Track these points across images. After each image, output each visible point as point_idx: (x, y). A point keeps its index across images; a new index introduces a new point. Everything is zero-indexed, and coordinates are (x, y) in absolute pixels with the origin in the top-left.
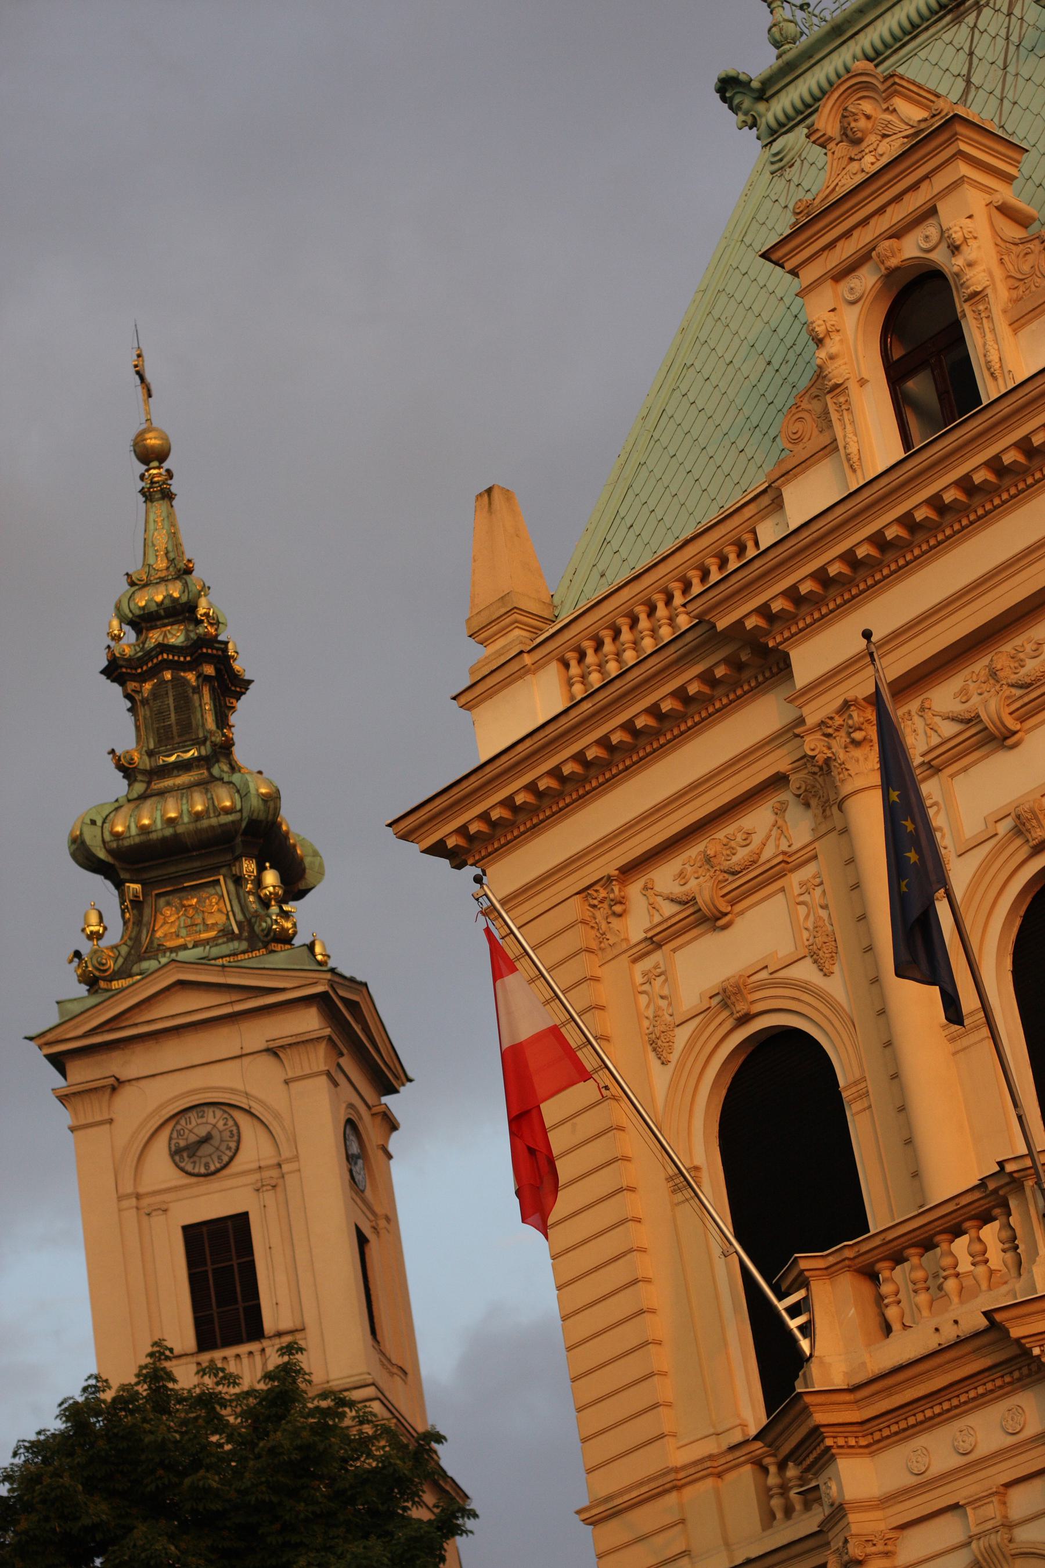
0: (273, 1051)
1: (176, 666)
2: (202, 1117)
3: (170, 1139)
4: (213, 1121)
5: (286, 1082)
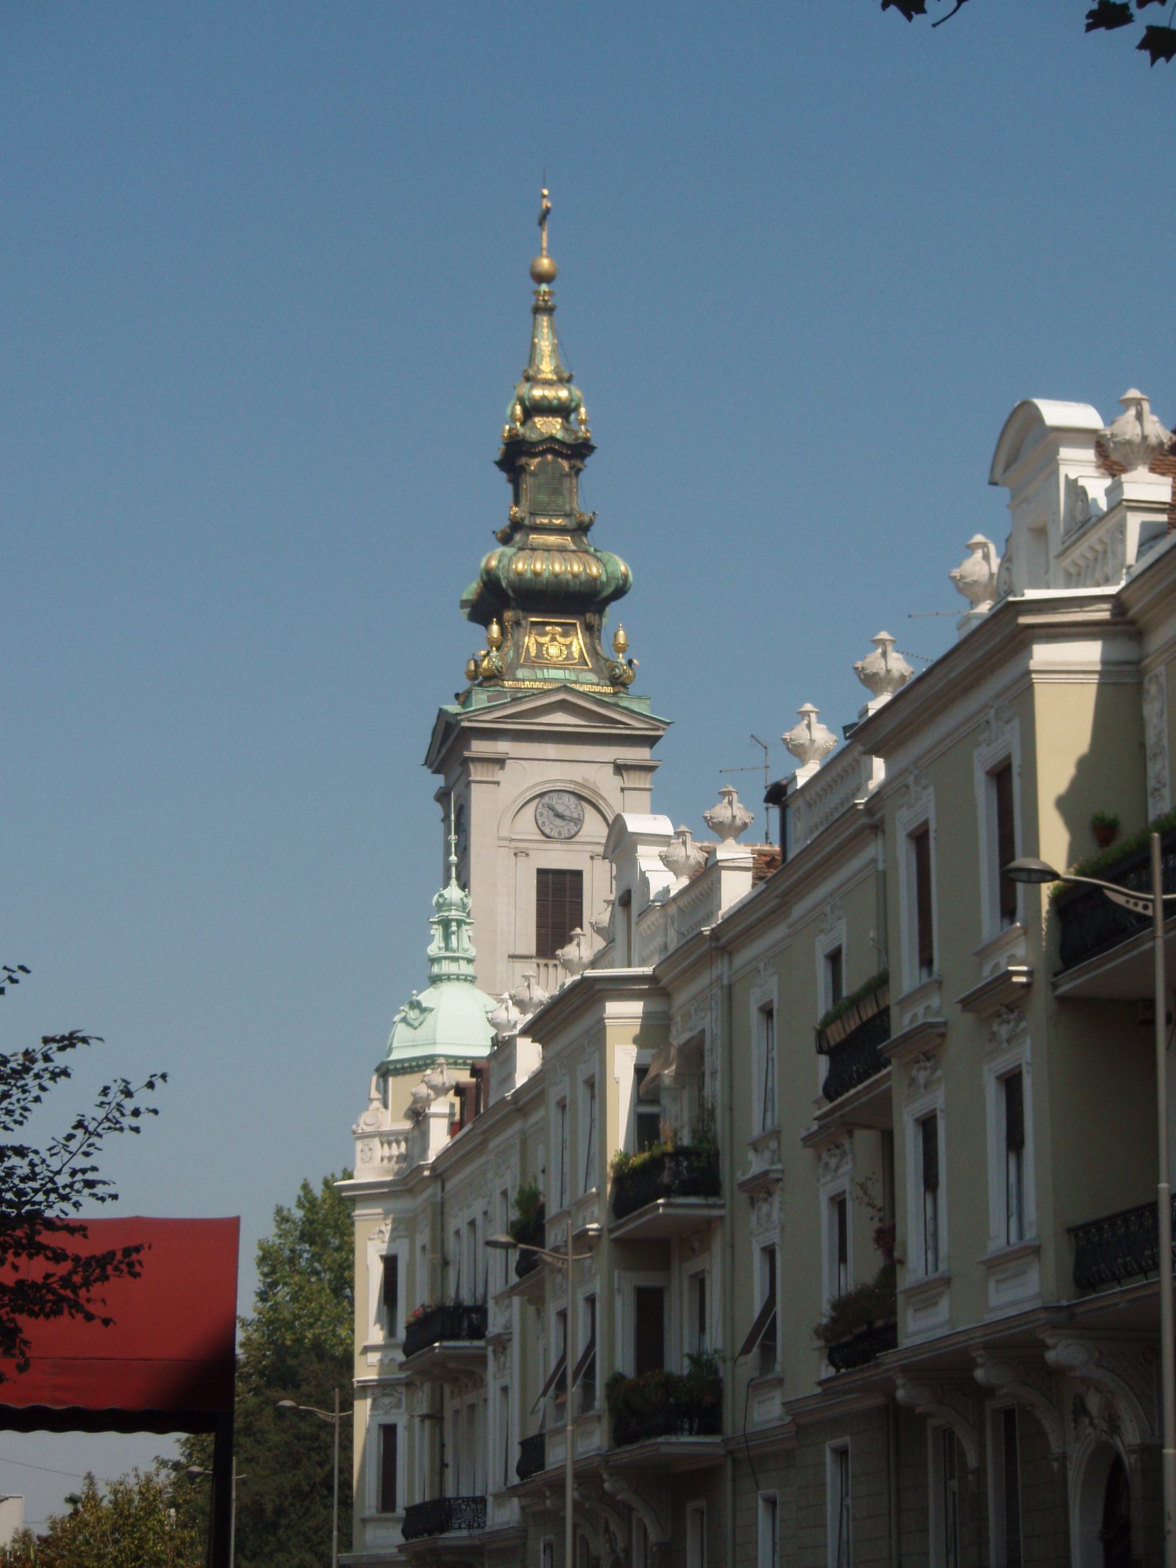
0: (620, 769)
1: (557, 454)
2: (561, 799)
3: (537, 808)
4: (568, 804)
5: (622, 790)
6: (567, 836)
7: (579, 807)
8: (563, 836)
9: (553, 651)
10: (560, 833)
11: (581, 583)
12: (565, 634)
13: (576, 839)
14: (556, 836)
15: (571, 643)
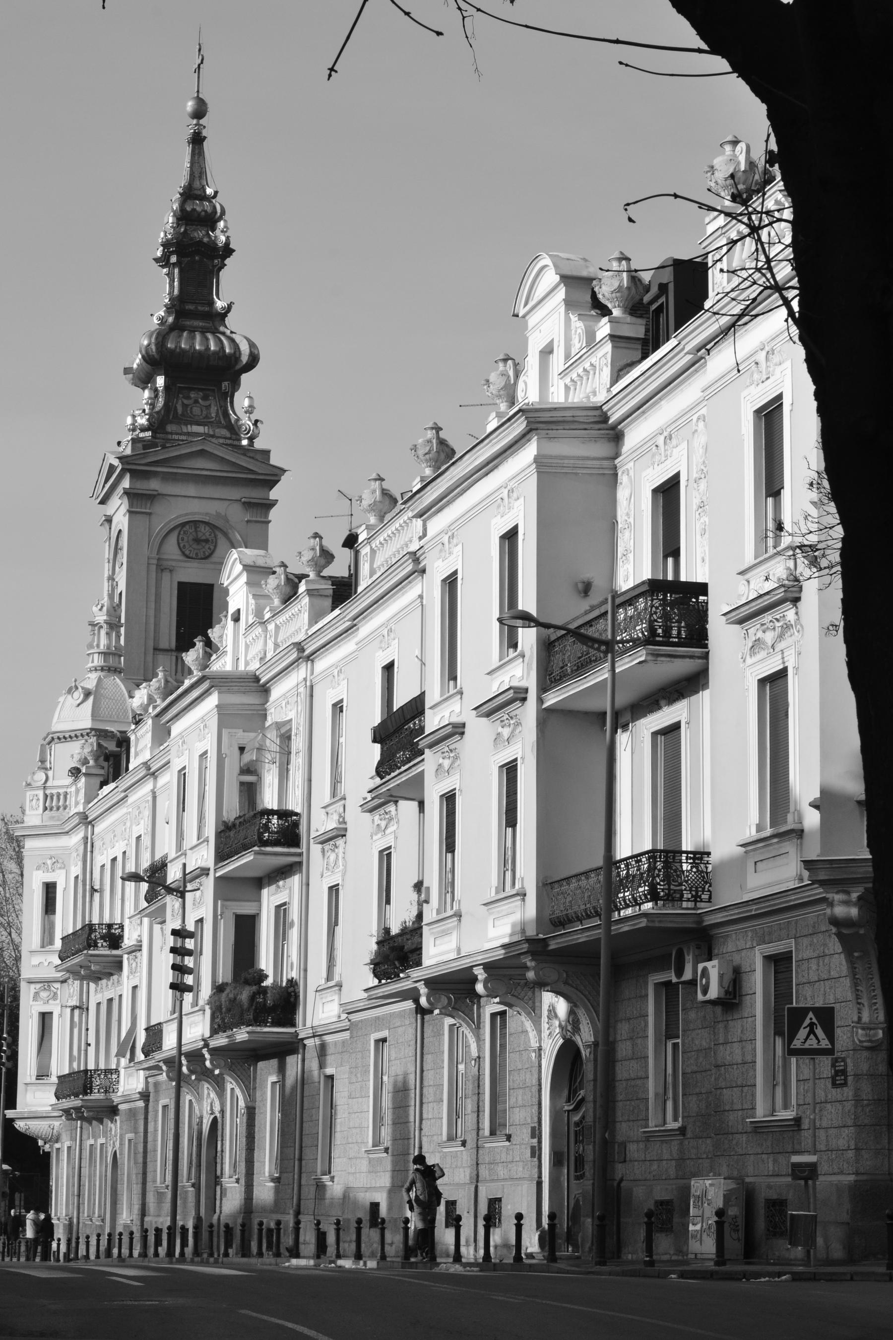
3: (179, 534)
8: (199, 557)
9: (196, 410)
10: (197, 554)
12: (205, 398)
14: (194, 556)
15: (210, 405)
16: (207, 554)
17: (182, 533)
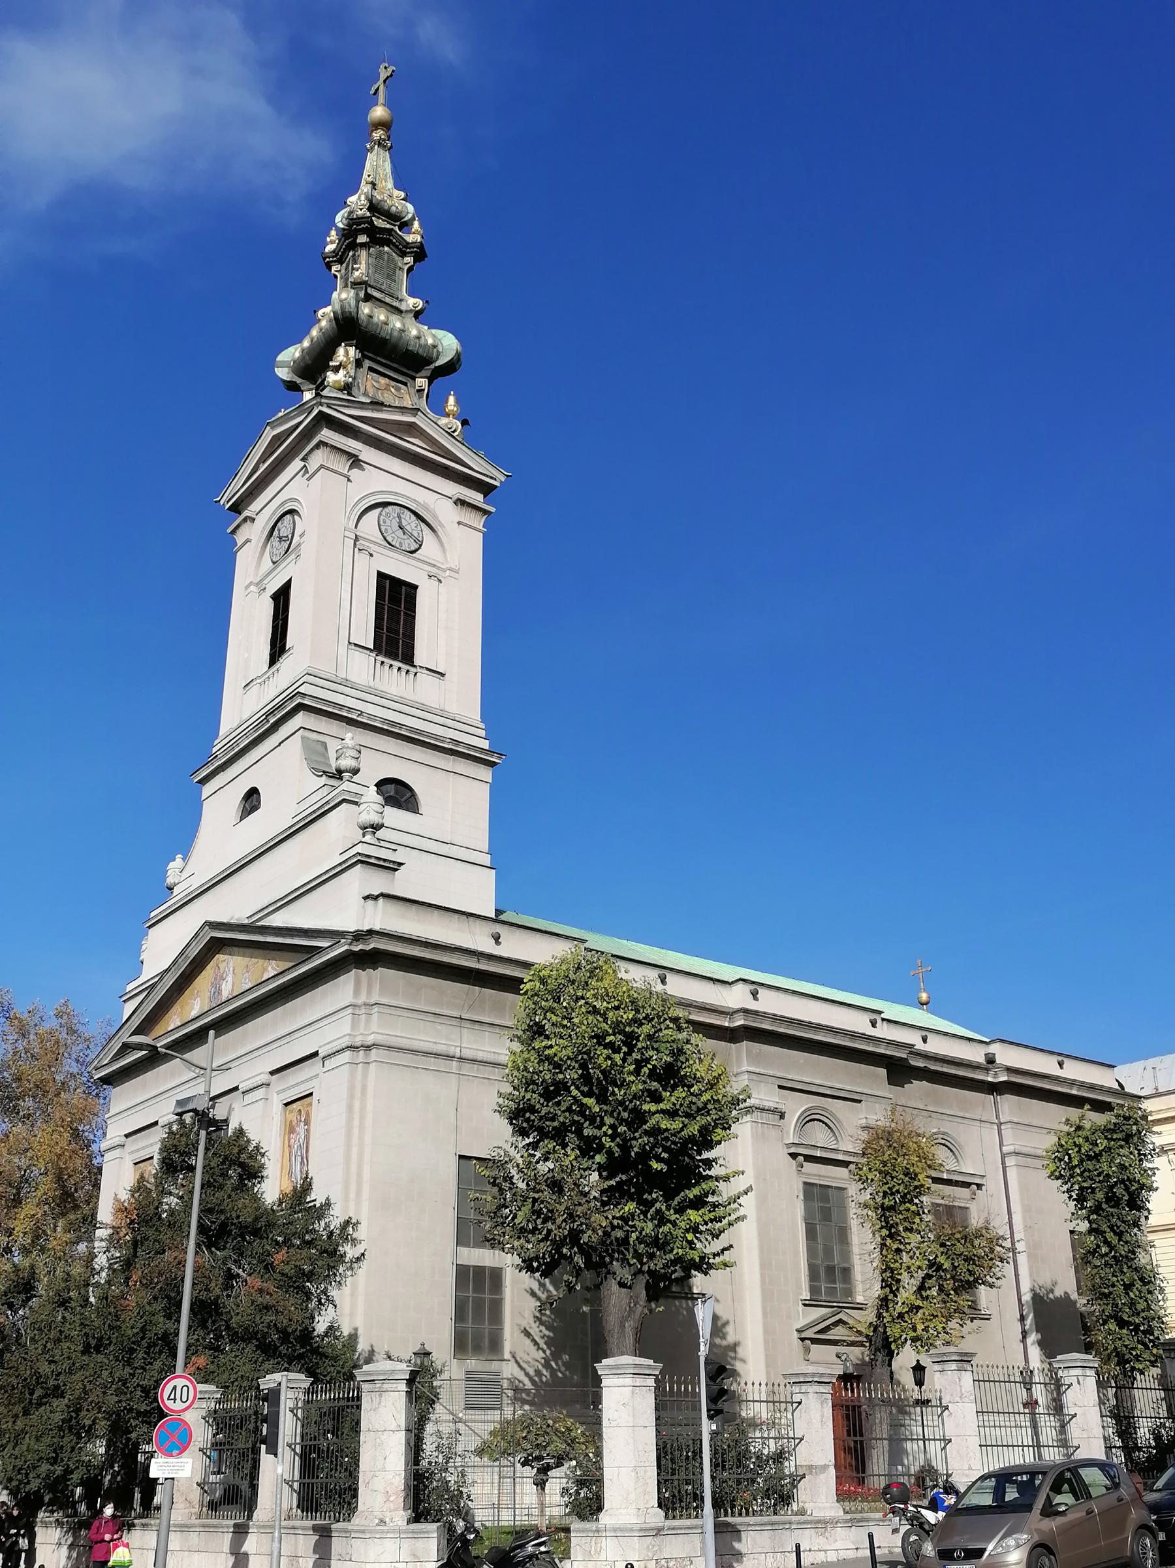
3: (380, 514)
6: (408, 550)
7: (419, 527)
10: (400, 543)
11: (420, 346)
13: (414, 555)
14: (398, 546)
16: (413, 548)
17: (384, 513)
